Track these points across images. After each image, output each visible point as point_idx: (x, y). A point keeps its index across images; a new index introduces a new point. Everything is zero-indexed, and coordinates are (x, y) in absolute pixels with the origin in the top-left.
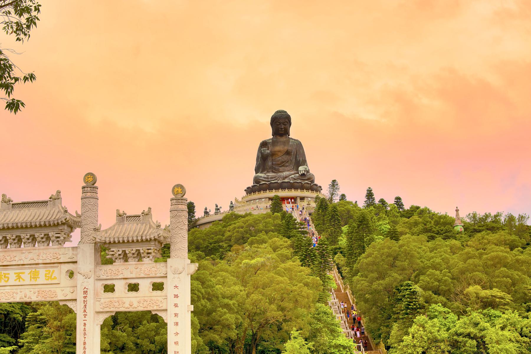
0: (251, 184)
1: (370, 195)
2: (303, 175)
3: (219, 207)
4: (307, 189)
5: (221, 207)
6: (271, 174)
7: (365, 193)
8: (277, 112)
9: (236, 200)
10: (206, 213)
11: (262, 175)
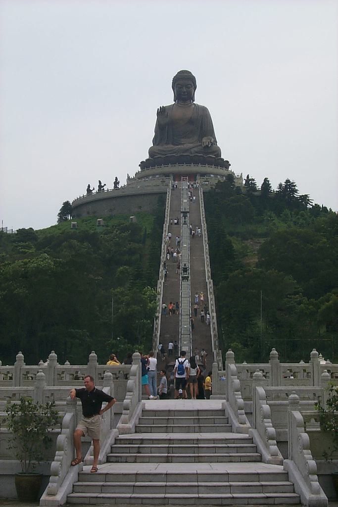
0: (146, 156)
2: (207, 146)
3: (102, 185)
4: (210, 164)
5: (105, 185)
6: (170, 146)
10: (89, 191)
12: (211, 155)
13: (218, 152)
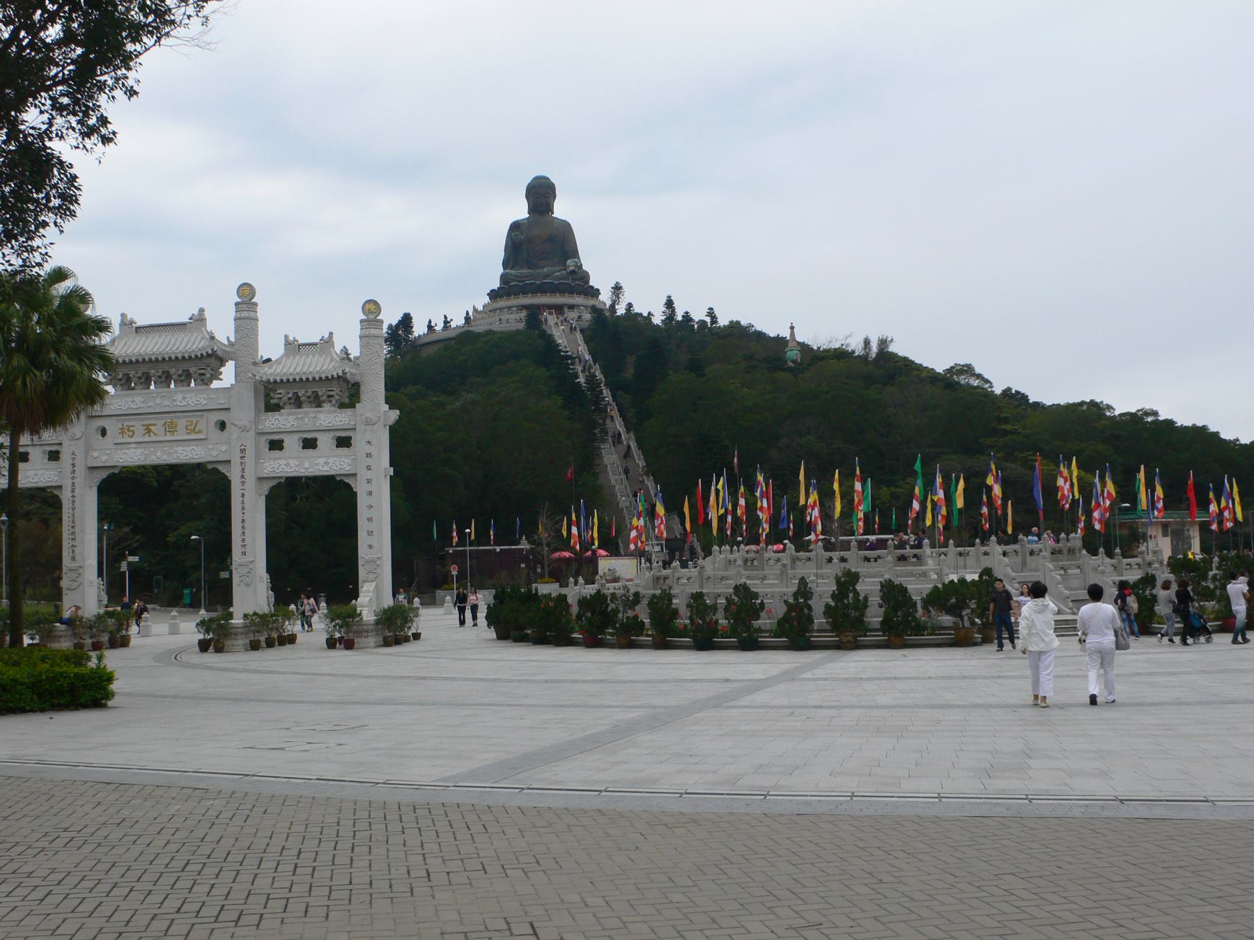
0: (496, 284)
1: (669, 304)
2: (573, 272)
4: (579, 293)
7: (664, 300)
8: (536, 178)
9: (475, 309)
10: (430, 327)
11: (513, 272)
12: (580, 284)
13: (585, 277)
